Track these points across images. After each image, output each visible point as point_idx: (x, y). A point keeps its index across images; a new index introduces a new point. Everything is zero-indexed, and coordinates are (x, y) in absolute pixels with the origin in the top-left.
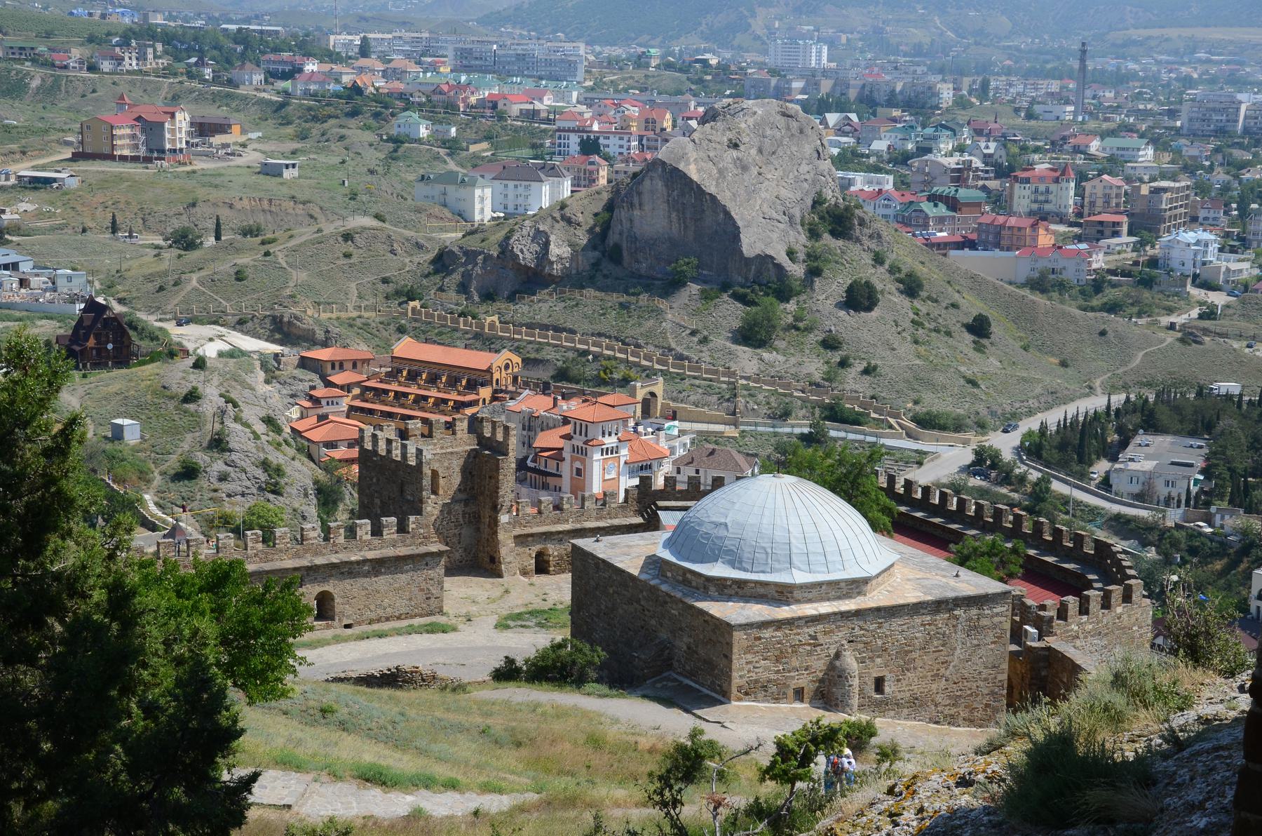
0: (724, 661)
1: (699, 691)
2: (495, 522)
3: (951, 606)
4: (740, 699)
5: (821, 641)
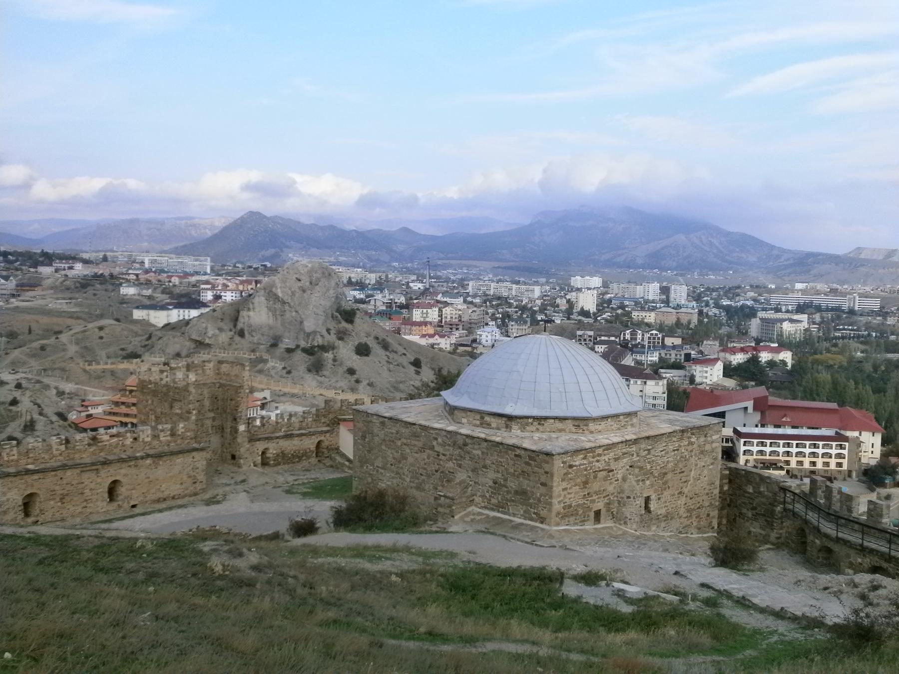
0: (543, 490)
1: (511, 521)
2: (236, 431)
3: (689, 434)
4: (558, 524)
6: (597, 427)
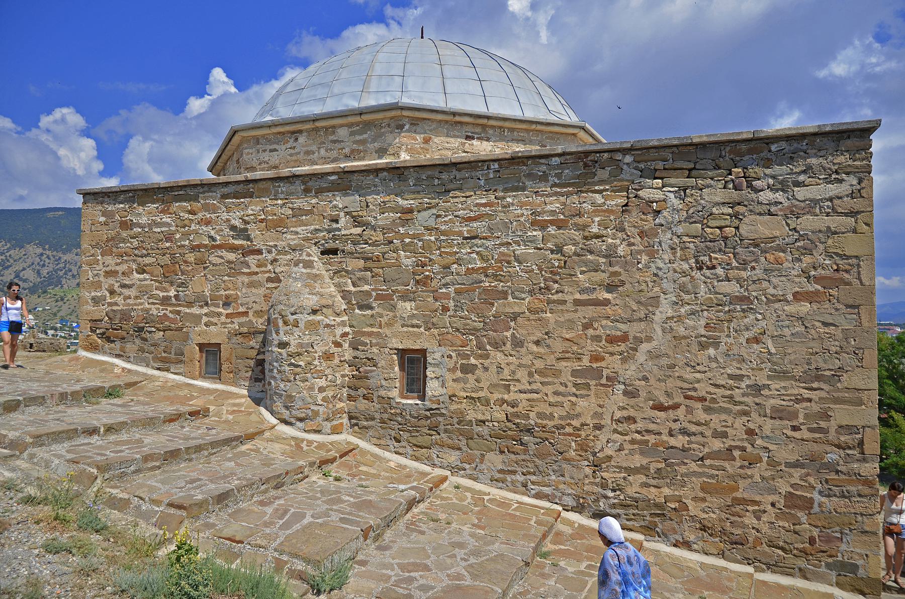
4: (93, 348)
5: (258, 244)
6: (266, 156)
